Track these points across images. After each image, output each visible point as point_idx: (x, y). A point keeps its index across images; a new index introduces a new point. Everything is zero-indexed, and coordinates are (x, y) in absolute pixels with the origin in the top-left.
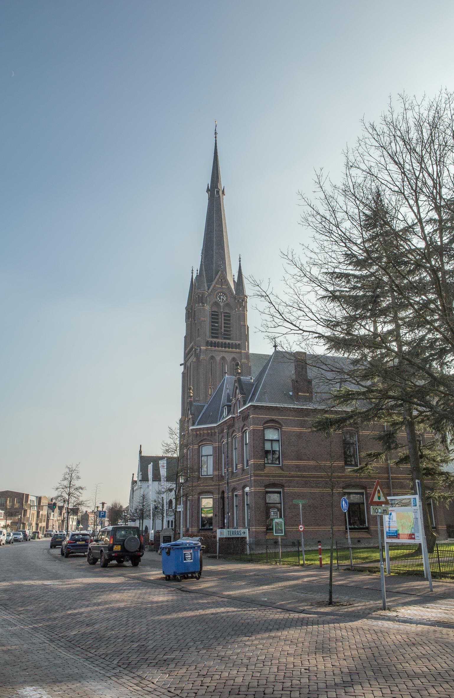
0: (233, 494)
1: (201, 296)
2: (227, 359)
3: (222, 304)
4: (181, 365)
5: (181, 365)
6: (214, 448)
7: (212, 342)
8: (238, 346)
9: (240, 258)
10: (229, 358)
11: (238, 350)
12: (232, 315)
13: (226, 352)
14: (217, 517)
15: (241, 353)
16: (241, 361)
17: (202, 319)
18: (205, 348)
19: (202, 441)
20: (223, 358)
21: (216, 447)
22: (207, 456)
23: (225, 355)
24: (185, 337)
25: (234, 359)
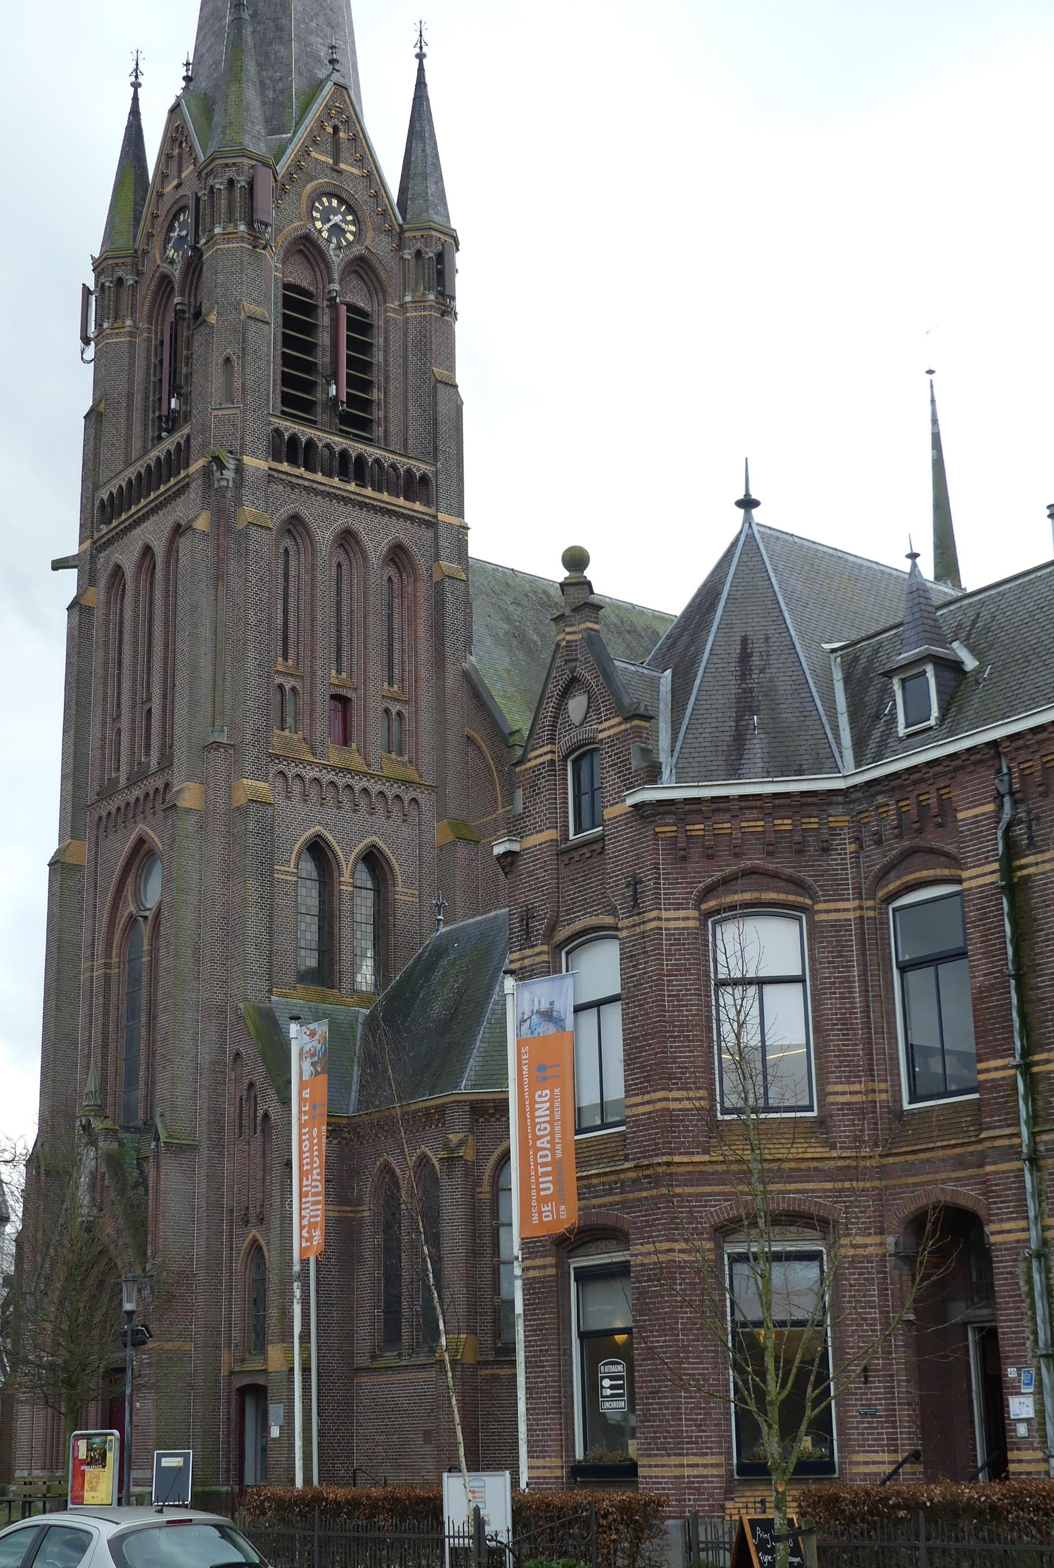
0: (719, 1250)
1: (242, 182)
2: (369, 546)
3: (336, 259)
4: (58, 565)
5: (58, 565)
6: (816, 937)
7: (294, 439)
8: (416, 487)
9: (421, 43)
10: (377, 538)
11: (418, 506)
12: (379, 322)
13: (362, 505)
14: (877, 1384)
15: (432, 524)
16: (423, 568)
17: (250, 308)
18: (263, 465)
19: (726, 882)
20: (347, 539)
21: (838, 926)
22: (761, 982)
23: (360, 522)
24: (94, 418)
25: (398, 555)
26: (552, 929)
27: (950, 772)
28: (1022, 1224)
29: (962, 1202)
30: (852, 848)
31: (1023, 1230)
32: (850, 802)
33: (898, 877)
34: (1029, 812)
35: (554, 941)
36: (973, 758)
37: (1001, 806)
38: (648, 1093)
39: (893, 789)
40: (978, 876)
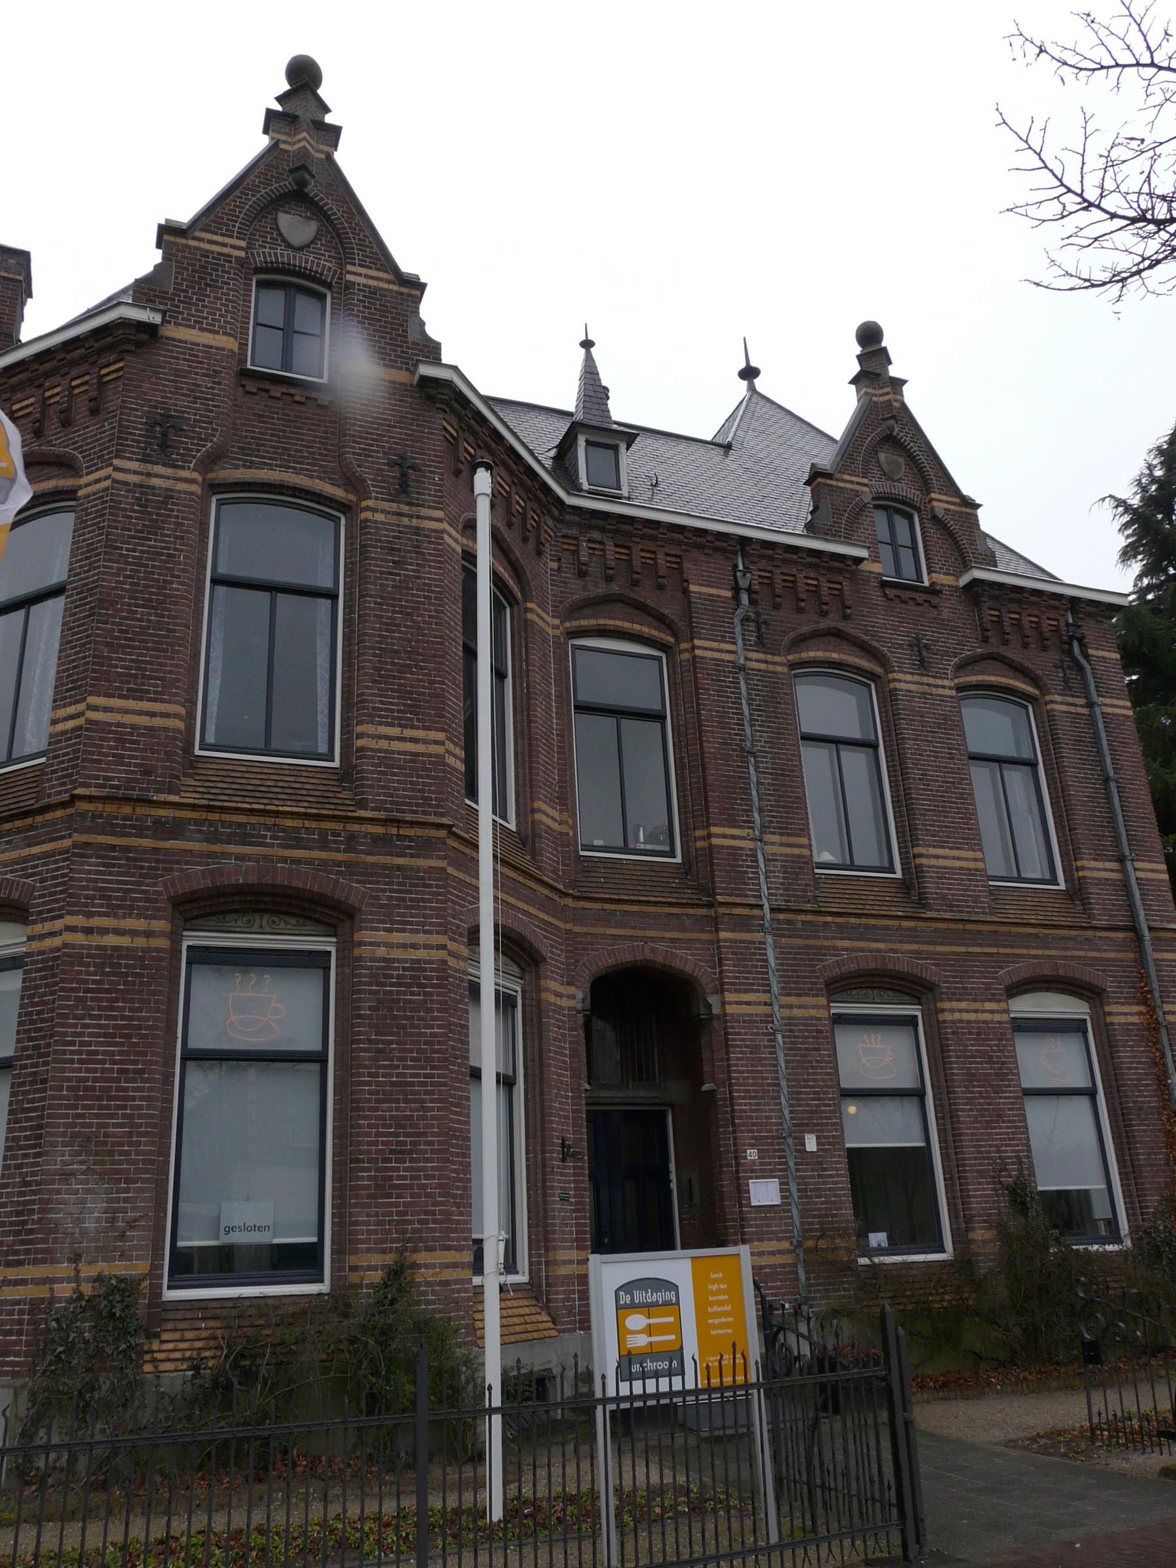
26: (213, 460)
27: (687, 544)
28: (764, 997)
29: (677, 964)
30: (555, 565)
31: (766, 1004)
32: (562, 522)
33: (595, 617)
34: (758, 614)
35: (210, 476)
36: (718, 543)
37: (736, 597)
38: (413, 727)
39: (616, 531)
40: (712, 649)
